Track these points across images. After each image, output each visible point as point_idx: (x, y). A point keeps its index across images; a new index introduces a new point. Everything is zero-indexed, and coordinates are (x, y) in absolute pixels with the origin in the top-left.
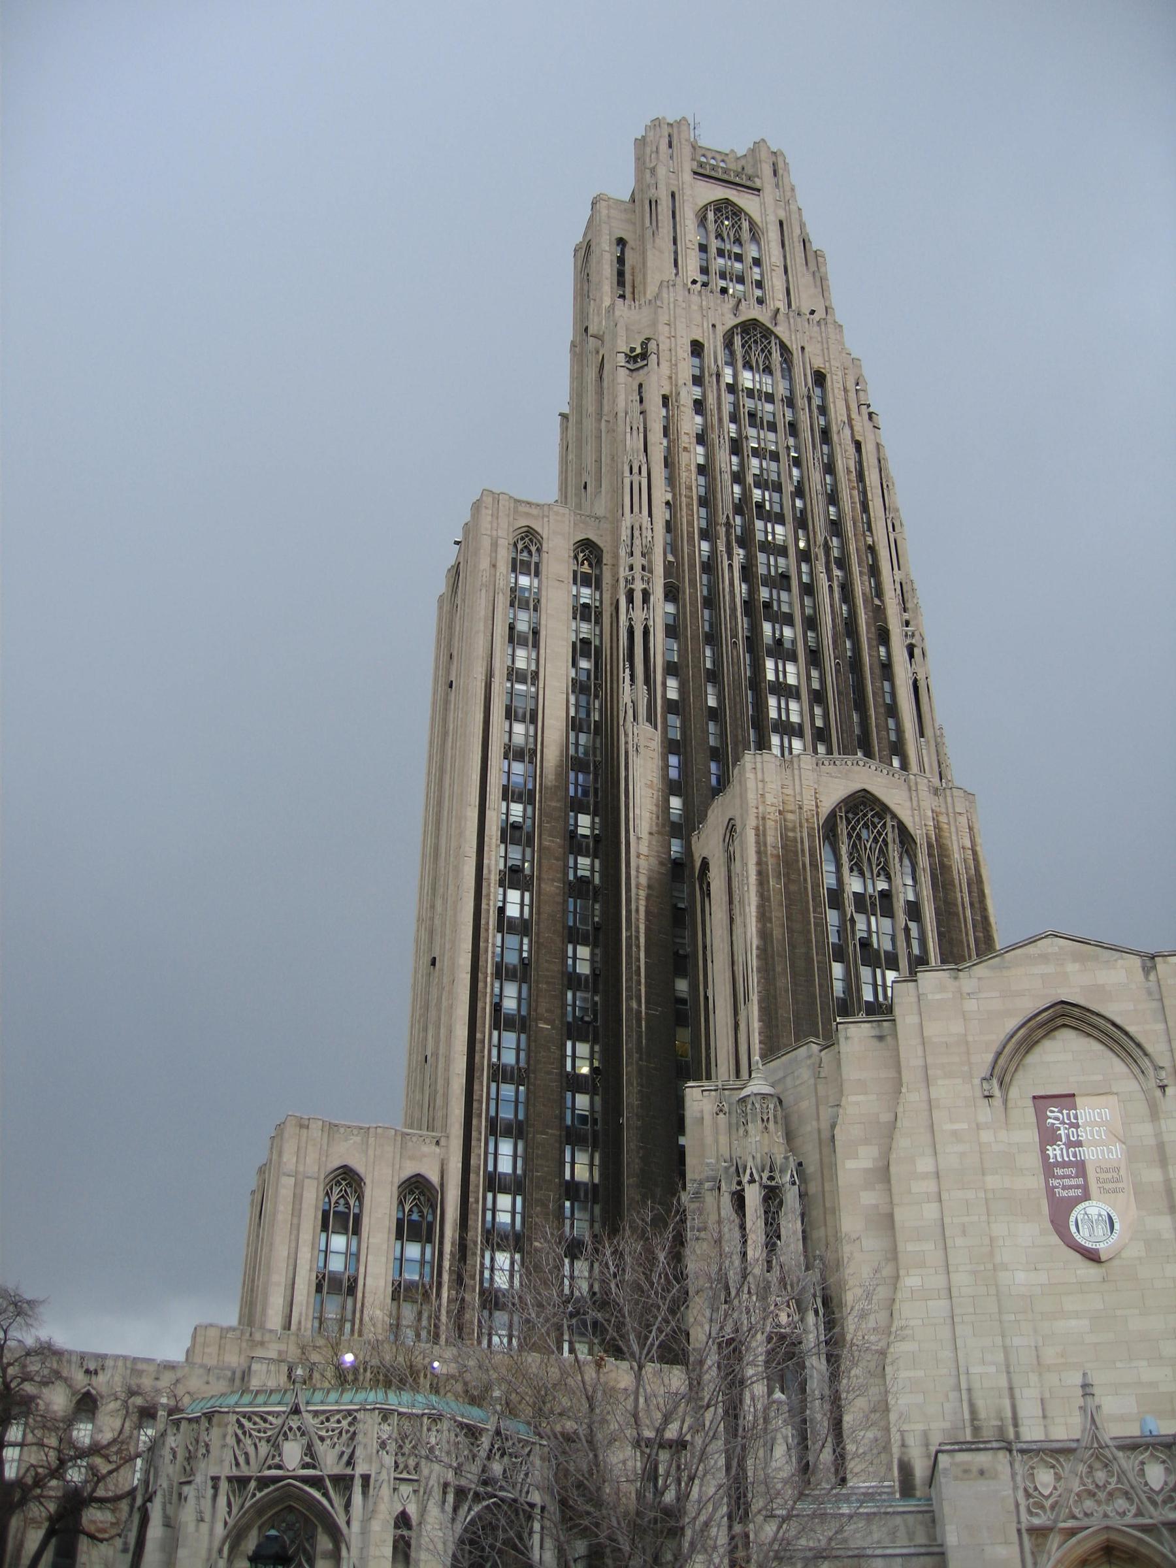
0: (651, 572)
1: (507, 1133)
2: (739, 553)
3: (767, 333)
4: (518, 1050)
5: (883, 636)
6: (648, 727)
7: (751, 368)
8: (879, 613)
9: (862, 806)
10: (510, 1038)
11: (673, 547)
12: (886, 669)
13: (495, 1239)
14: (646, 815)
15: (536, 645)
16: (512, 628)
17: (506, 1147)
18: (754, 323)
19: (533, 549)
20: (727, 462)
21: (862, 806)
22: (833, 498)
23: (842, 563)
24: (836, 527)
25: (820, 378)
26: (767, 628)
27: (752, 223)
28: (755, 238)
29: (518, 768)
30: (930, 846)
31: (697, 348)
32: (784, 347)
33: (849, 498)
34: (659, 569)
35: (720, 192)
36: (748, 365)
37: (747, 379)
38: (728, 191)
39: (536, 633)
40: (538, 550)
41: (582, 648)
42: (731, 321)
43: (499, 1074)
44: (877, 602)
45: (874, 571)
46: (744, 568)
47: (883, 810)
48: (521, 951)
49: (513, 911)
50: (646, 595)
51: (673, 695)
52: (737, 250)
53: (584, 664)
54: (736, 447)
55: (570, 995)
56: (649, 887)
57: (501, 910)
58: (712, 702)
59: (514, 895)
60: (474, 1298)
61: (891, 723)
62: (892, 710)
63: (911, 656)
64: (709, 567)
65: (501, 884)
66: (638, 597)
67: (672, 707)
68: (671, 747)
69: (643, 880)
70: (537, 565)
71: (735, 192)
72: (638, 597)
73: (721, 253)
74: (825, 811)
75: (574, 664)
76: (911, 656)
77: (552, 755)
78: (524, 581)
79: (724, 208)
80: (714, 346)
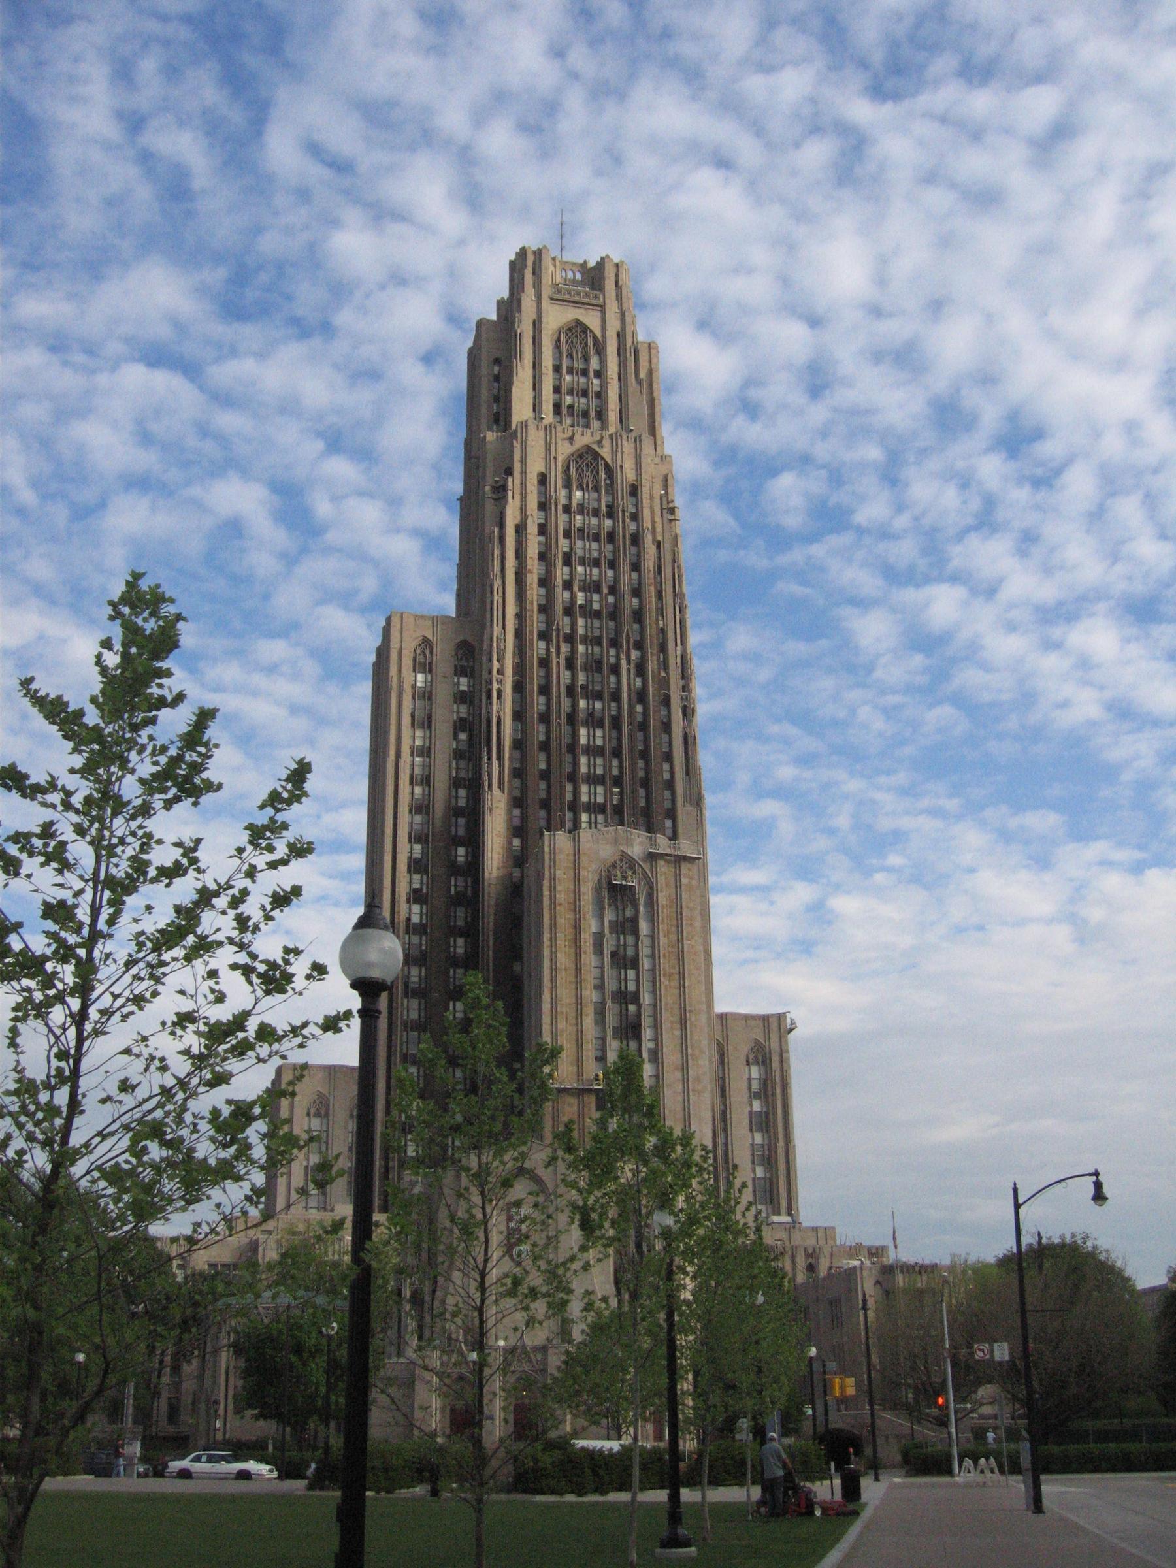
0: (503, 674)
2: (565, 648)
3: (596, 456)
4: (420, 1010)
5: (666, 701)
6: (496, 792)
7: (582, 489)
8: (664, 683)
10: (414, 1003)
12: (667, 727)
14: (496, 856)
20: (561, 573)
22: (637, 592)
23: (639, 645)
24: (638, 616)
25: (634, 491)
26: (582, 704)
33: (650, 592)
35: (571, 314)
38: (577, 310)
41: (461, 725)
43: (408, 1026)
44: (663, 674)
45: (663, 648)
46: (567, 659)
48: (421, 945)
49: (415, 919)
50: (499, 692)
53: (463, 736)
54: (568, 560)
55: (452, 971)
56: (497, 905)
57: (408, 920)
58: (543, 766)
59: (416, 908)
61: (666, 767)
62: (668, 757)
64: (544, 663)
65: (408, 901)
69: (492, 902)
70: (430, 664)
71: (582, 311)
75: (455, 737)
77: (439, 809)
79: (578, 329)
80: (557, 477)
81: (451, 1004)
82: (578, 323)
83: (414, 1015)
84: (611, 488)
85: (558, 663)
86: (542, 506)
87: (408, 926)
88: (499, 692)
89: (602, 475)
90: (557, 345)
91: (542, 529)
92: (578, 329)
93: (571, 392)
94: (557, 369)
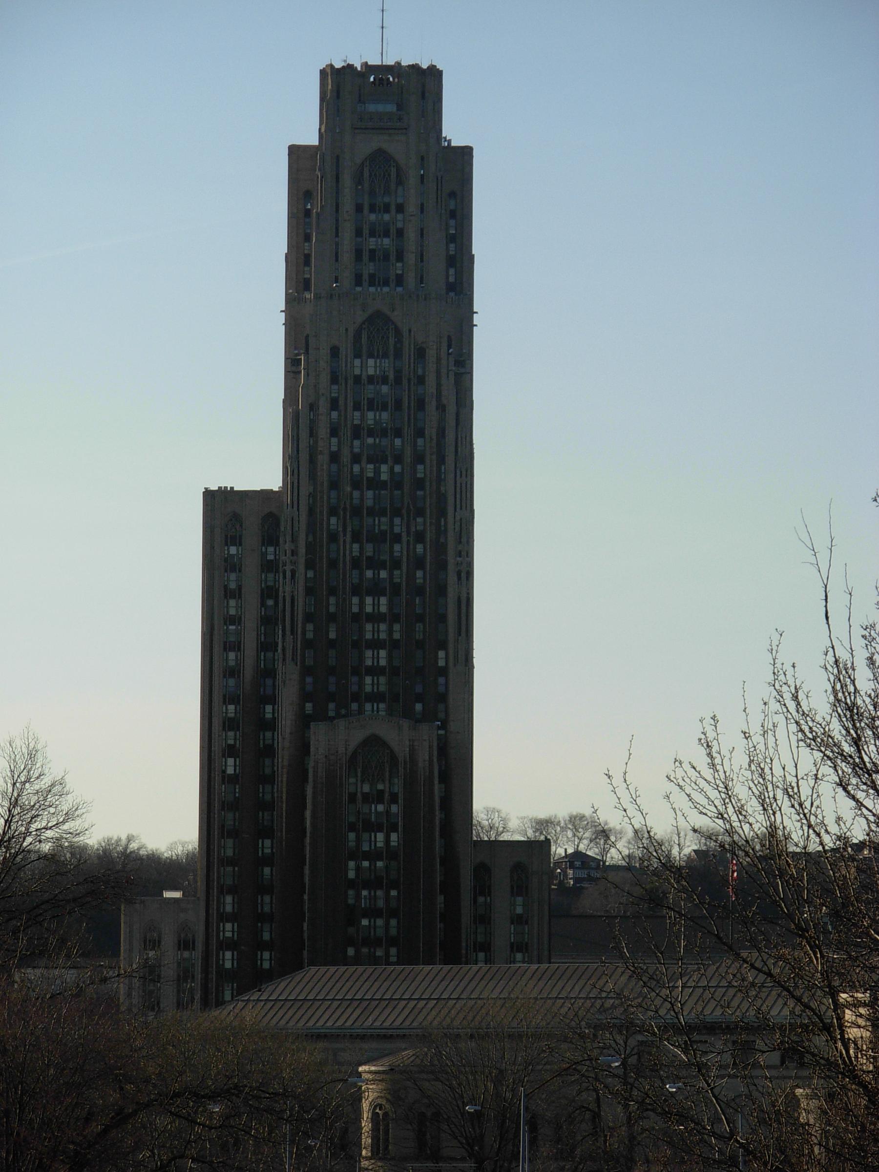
1: (229, 892)
9: (373, 742)
10: (230, 842)
11: (312, 527)
13: (224, 945)
15: (240, 597)
16: (226, 587)
17: (229, 899)
18: (378, 314)
19: (238, 527)
21: (373, 742)
27: (399, 169)
28: (400, 182)
29: (232, 682)
30: (405, 762)
31: (335, 352)
32: (398, 332)
34: (302, 550)
36: (371, 356)
37: (372, 367)
39: (240, 588)
40: (241, 526)
42: (360, 317)
47: (384, 744)
48: (235, 792)
49: (230, 771)
50: (293, 573)
51: (310, 635)
52: (386, 200)
53: (270, 602)
55: (261, 813)
57: (224, 772)
59: (231, 761)
60: (213, 976)
63: (459, 578)
66: (288, 574)
67: (308, 644)
68: (306, 671)
69: (286, 763)
72: (288, 574)
73: (372, 209)
74: (351, 748)
75: (263, 604)
76: (459, 578)
77: (248, 672)
78: (233, 550)
79: (380, 157)
81: (260, 841)
82: (380, 152)
83: (230, 853)
84: (398, 354)
85: (344, 541)
86: (334, 380)
87: (223, 778)
88: (293, 573)
89: (392, 341)
90: (358, 179)
91: (334, 404)
92: (380, 157)
93: (372, 234)
94: (359, 208)
